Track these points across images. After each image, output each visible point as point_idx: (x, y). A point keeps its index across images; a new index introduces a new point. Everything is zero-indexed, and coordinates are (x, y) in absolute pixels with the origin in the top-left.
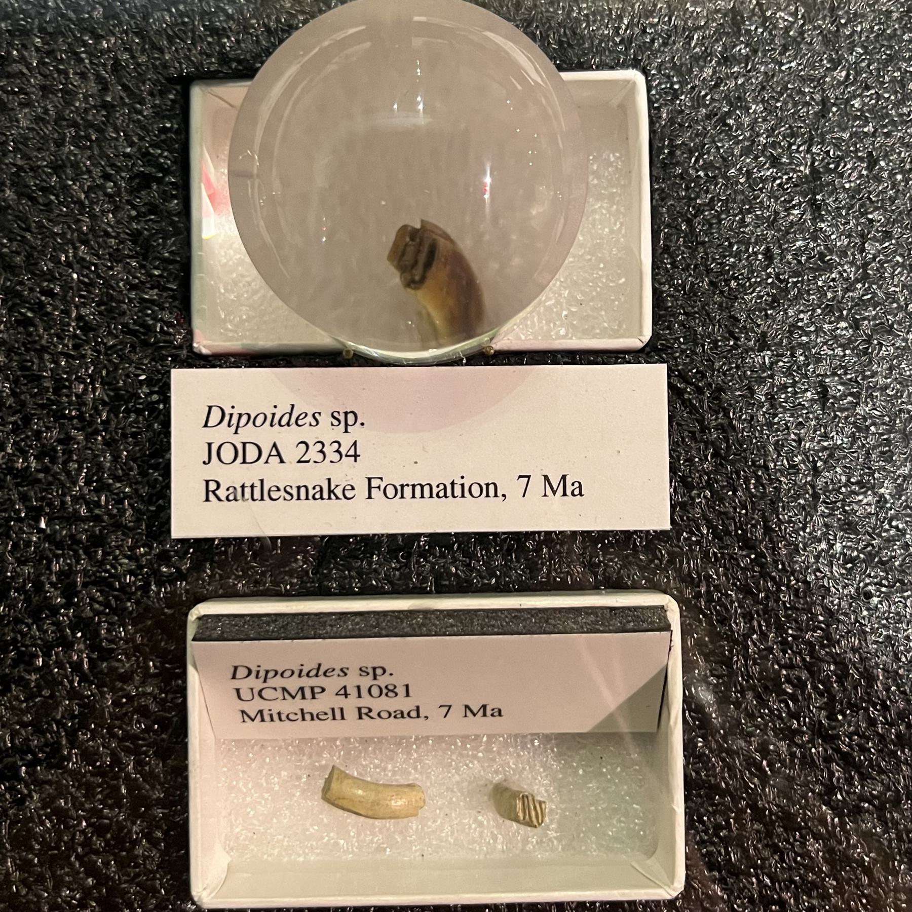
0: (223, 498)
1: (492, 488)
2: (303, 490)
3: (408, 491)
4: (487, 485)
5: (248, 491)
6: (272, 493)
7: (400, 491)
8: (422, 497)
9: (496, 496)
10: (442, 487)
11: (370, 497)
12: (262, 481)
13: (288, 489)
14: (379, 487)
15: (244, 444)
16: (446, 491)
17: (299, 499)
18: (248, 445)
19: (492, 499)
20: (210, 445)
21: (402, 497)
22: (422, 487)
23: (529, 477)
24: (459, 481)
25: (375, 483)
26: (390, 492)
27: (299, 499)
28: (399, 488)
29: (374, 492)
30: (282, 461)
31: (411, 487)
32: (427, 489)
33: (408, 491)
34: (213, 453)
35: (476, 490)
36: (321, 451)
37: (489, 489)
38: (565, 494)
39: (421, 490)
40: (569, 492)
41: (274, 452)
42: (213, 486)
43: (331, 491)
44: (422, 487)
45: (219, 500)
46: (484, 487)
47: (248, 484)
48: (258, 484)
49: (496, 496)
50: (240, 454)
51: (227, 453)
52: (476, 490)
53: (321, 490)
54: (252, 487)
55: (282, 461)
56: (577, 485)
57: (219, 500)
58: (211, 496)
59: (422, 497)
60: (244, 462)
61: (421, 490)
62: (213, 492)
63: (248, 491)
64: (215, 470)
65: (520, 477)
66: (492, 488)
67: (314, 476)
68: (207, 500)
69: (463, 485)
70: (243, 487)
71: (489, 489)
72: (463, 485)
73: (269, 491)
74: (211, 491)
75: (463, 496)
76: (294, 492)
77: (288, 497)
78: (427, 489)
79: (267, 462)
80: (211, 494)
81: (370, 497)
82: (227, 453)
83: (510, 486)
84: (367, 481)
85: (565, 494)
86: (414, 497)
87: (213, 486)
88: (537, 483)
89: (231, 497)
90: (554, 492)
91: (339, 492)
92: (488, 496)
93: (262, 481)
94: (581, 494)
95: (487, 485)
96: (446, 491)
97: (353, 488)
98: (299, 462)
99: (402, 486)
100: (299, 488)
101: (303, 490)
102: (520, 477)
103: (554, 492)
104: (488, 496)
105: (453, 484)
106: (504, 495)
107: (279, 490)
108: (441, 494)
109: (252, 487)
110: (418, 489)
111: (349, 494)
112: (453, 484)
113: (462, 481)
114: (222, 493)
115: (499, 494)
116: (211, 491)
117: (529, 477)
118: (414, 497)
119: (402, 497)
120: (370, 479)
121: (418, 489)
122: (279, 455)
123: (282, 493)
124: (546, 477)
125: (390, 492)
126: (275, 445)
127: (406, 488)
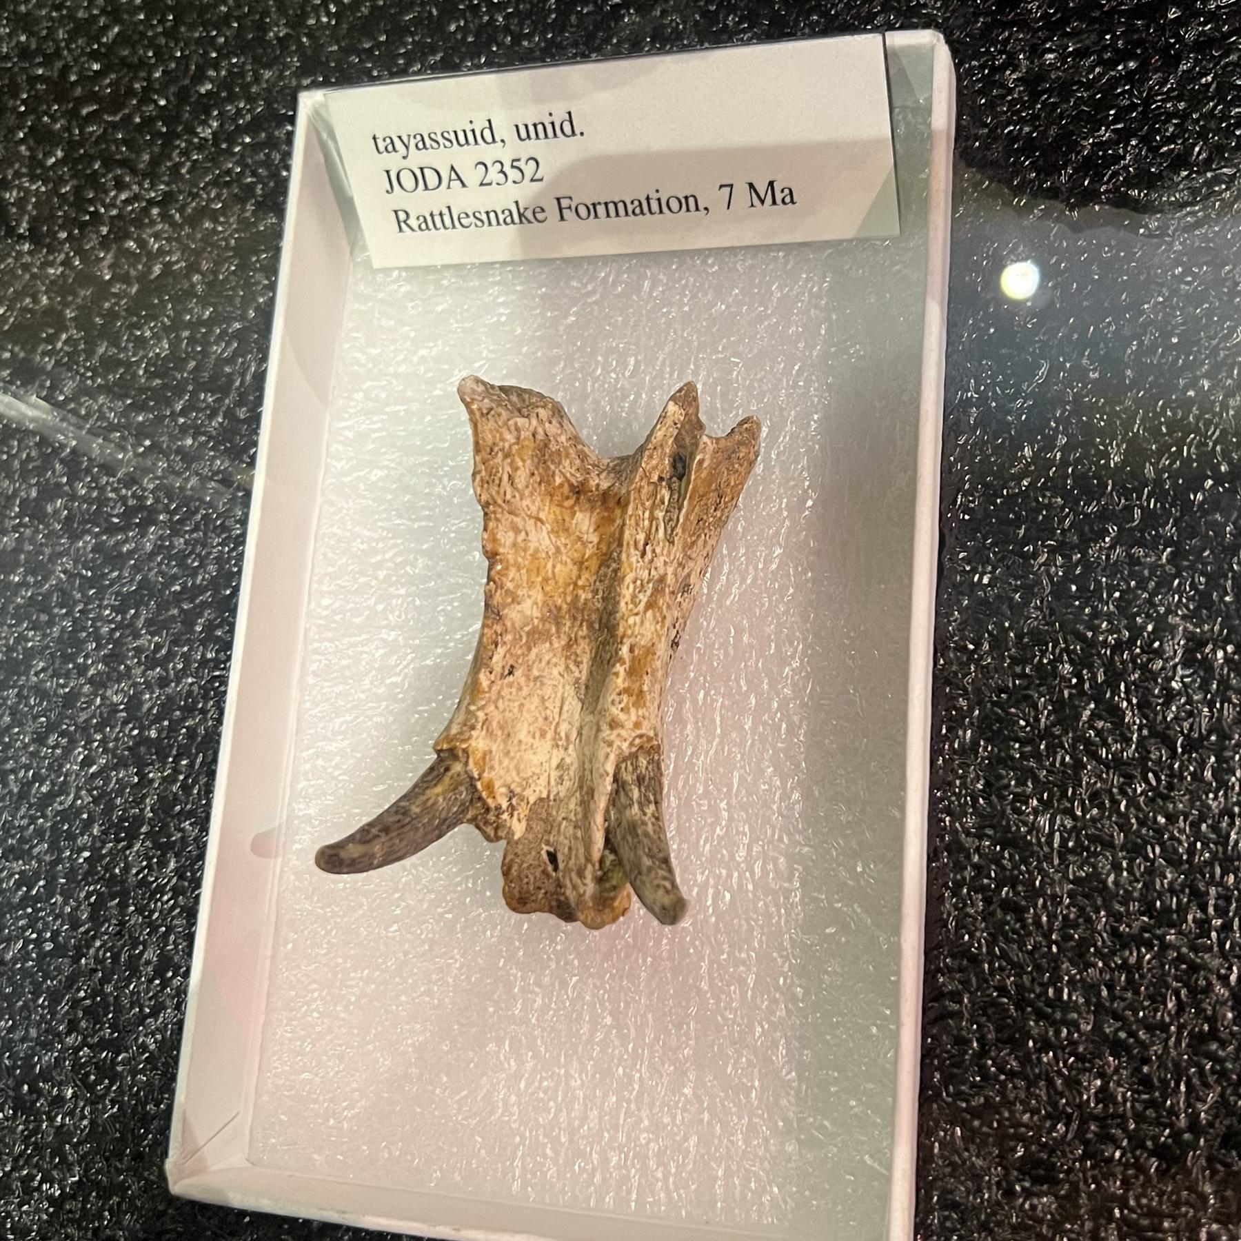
0: (415, 226)
1: (691, 200)
2: (492, 215)
4: (686, 198)
5: (437, 219)
6: (463, 221)
7: (592, 209)
8: (617, 215)
9: (697, 209)
10: (636, 203)
11: (562, 218)
12: (449, 208)
14: (570, 208)
15: (422, 169)
17: (490, 224)
19: (693, 213)
20: (388, 172)
22: (616, 204)
23: (731, 186)
24: (654, 196)
25: (565, 203)
27: (490, 224)
29: (566, 213)
30: (464, 185)
31: (603, 206)
32: (621, 206)
34: (393, 180)
35: (674, 205)
36: (502, 171)
37: (688, 203)
38: (774, 202)
42: (402, 216)
43: (520, 215)
44: (616, 204)
46: (683, 201)
47: (436, 212)
48: (445, 211)
49: (697, 209)
50: (419, 177)
52: (674, 205)
54: (441, 214)
55: (464, 185)
56: (787, 191)
58: (403, 225)
59: (617, 215)
60: (426, 188)
61: (615, 208)
62: (405, 222)
63: (437, 219)
64: (399, 199)
65: (721, 186)
66: (691, 200)
69: (659, 200)
70: (432, 215)
71: (688, 203)
72: (659, 200)
74: (401, 220)
75: (661, 212)
76: (484, 217)
77: (479, 223)
78: (621, 206)
79: (449, 187)
80: (403, 225)
81: (562, 218)
83: (710, 196)
84: (555, 202)
85: (774, 202)
86: (608, 215)
87: (402, 216)
88: (741, 192)
89: (423, 226)
90: (762, 202)
91: (529, 214)
92: (688, 210)
93: (449, 208)
94: (792, 202)
95: (686, 198)
96: (642, 207)
97: (543, 210)
98: (482, 184)
99: (594, 205)
100: (487, 213)
101: (492, 215)
102: (721, 186)
103: (762, 202)
104: (688, 210)
105: (648, 199)
106: (706, 209)
107: (467, 216)
108: (638, 211)
109: (441, 214)
110: (611, 207)
111: (540, 216)
112: (648, 199)
114: (413, 222)
115: (701, 207)
117: (731, 186)
118: (608, 215)
120: (558, 199)
121: (611, 207)
122: (459, 178)
123: (472, 219)
124: (751, 185)
126: (452, 168)
127: (598, 207)
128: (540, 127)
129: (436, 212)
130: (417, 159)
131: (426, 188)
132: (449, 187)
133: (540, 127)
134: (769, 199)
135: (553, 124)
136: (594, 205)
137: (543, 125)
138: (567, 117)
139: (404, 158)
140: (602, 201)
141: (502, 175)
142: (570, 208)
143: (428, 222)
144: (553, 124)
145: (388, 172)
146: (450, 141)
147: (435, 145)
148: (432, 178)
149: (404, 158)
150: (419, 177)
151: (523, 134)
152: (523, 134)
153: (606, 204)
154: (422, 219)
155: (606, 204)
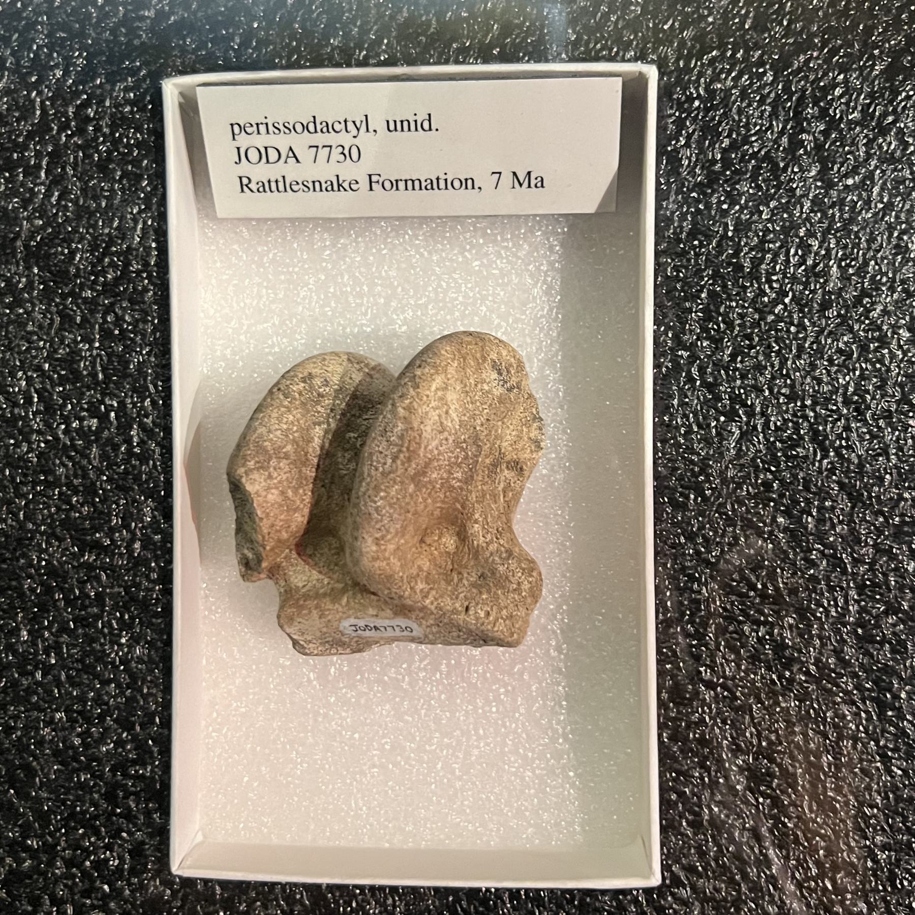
0: (255, 189)
1: (470, 182)
2: (317, 184)
3: (401, 185)
4: (466, 180)
5: (273, 185)
7: (395, 184)
9: (473, 188)
10: (429, 181)
11: (371, 189)
12: (284, 177)
13: (305, 183)
14: (378, 182)
15: (266, 148)
16: (432, 184)
17: (314, 190)
18: (269, 149)
19: (470, 191)
20: (238, 148)
21: (397, 189)
22: (413, 181)
24: (443, 177)
25: (374, 178)
26: (387, 185)
27: (314, 190)
28: (394, 183)
30: (298, 161)
32: (417, 183)
33: (401, 185)
34: (242, 155)
35: (457, 184)
37: (467, 183)
38: (529, 186)
39: (412, 184)
40: (532, 185)
41: (291, 154)
42: (245, 181)
43: (339, 185)
44: (413, 181)
45: (252, 191)
47: (273, 179)
48: (281, 179)
49: (473, 188)
50: (263, 154)
51: (253, 155)
52: (457, 184)
53: (332, 184)
54: (277, 181)
55: (298, 161)
56: (539, 179)
57: (252, 191)
58: (245, 188)
59: (414, 189)
60: (268, 162)
61: (412, 184)
63: (273, 185)
64: (245, 168)
66: (470, 182)
67: (325, 171)
68: (243, 191)
69: (446, 180)
70: (269, 182)
71: (467, 183)
72: (446, 180)
73: (291, 185)
74: (244, 184)
75: (446, 188)
76: (311, 185)
77: (306, 189)
78: (417, 183)
79: (286, 162)
80: (245, 188)
81: (371, 189)
82: (253, 155)
83: (485, 180)
85: (529, 186)
86: (406, 189)
87: (245, 181)
88: (507, 179)
89: (261, 189)
90: (521, 185)
91: (346, 185)
92: (466, 188)
93: (284, 177)
94: (542, 186)
95: (466, 180)
96: (432, 184)
97: (357, 183)
99: (397, 181)
100: (314, 182)
101: (317, 184)
104: (466, 188)
105: (438, 179)
106: (480, 188)
107: (298, 183)
108: (429, 187)
109: (277, 181)
110: (410, 183)
112: (438, 179)
113: (445, 177)
114: (253, 186)
115: (476, 186)
116: (244, 184)
117: (500, 173)
118: (406, 189)
119: (397, 189)
120: (370, 176)
121: (410, 183)
122: (295, 156)
123: (301, 186)
124: (514, 174)
125: (387, 185)
126: (291, 149)
127: (400, 183)
128: (405, 124)
129: (273, 179)
130: (261, 141)
131: (268, 162)
132: (286, 162)
133: (405, 124)
134: (526, 184)
135: (416, 121)
136: (397, 181)
137: (408, 121)
138: (427, 117)
139: (355, 137)
140: (403, 178)
141: (342, 156)
142: (378, 182)
143: (265, 187)
144: (416, 121)
145: (238, 148)
146: (289, 130)
147: (276, 131)
149: (355, 137)
150: (263, 154)
151: (392, 127)
152: (392, 127)
153: (406, 181)
154: (260, 184)
155: (406, 181)
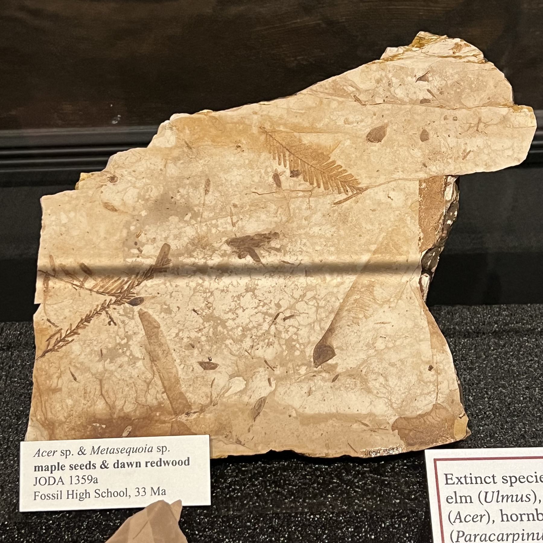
15: (49, 478)
20: (36, 478)
34: (38, 481)
38: (159, 495)
40: (160, 494)
50: (47, 481)
51: (43, 481)
55: (63, 484)
60: (49, 484)
64: (38, 487)
82: (43, 481)
85: (159, 495)
90: (155, 494)
103: (155, 494)
122: (62, 481)
124: (152, 488)
126: (61, 478)
148: (52, 481)
